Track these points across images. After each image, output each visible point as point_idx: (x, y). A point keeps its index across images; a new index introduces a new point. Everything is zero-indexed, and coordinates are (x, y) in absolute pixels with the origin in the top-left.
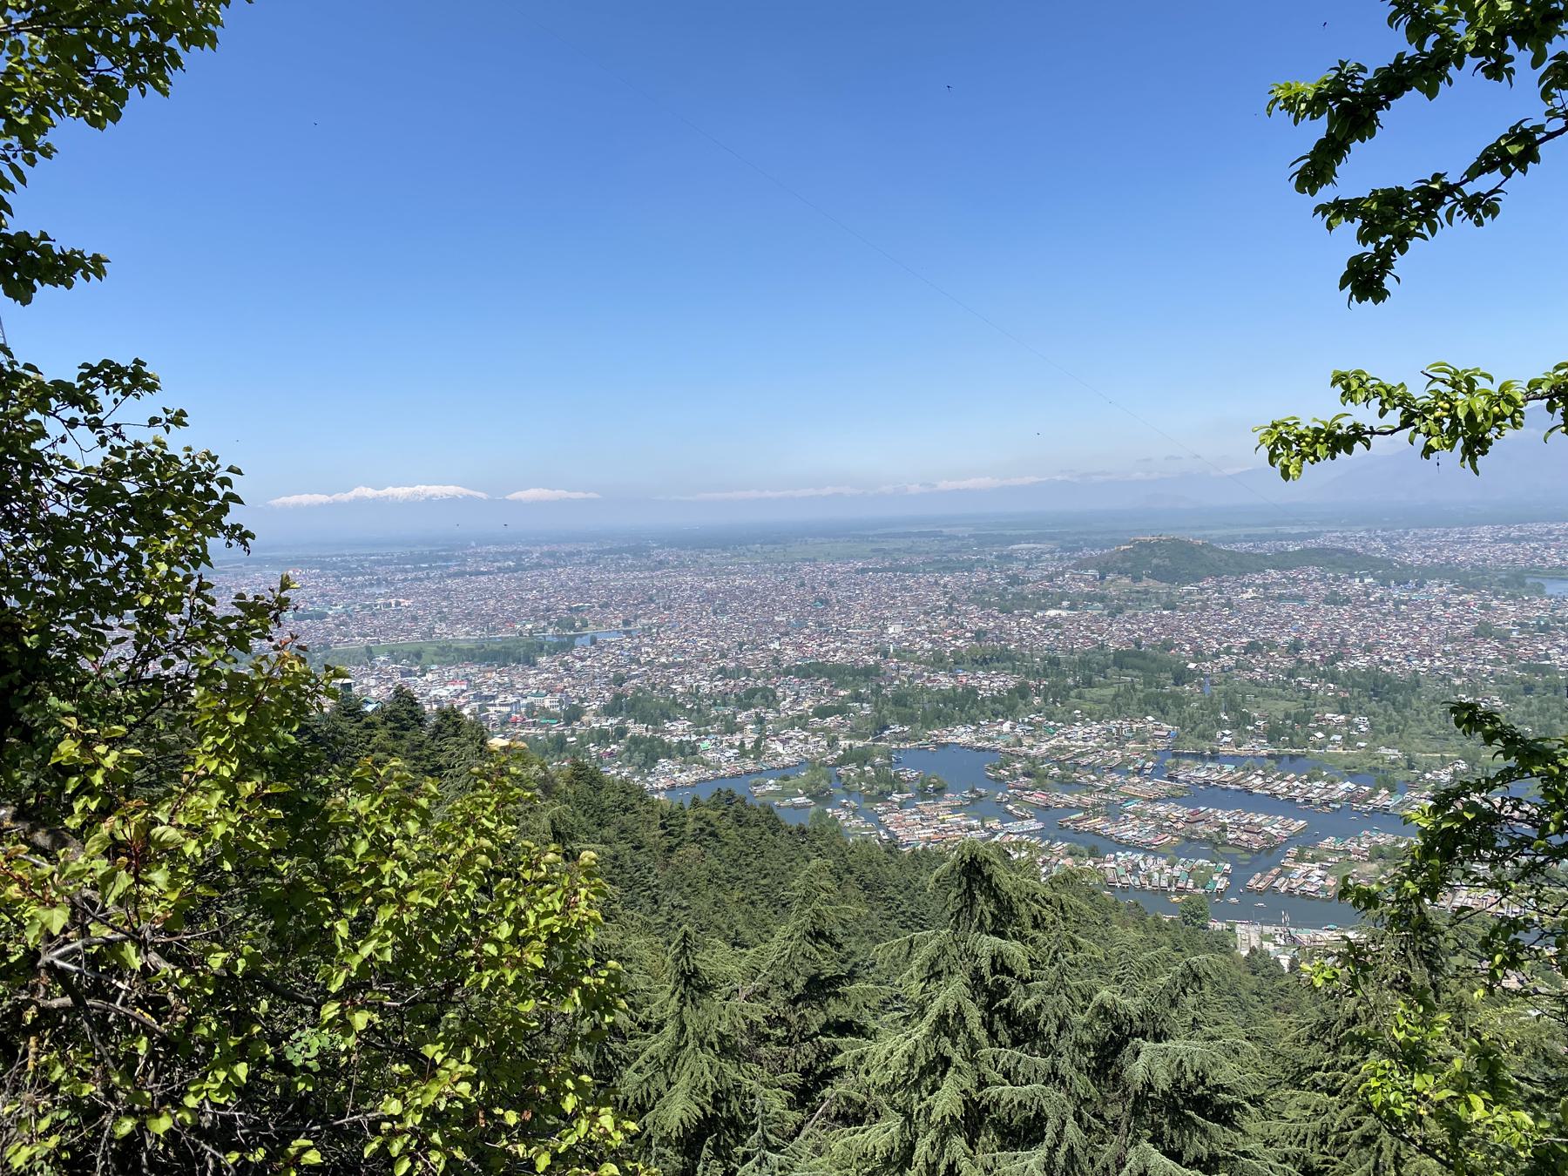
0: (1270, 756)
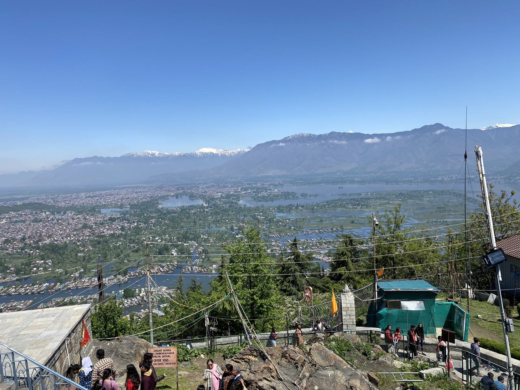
0: (17, 280)
